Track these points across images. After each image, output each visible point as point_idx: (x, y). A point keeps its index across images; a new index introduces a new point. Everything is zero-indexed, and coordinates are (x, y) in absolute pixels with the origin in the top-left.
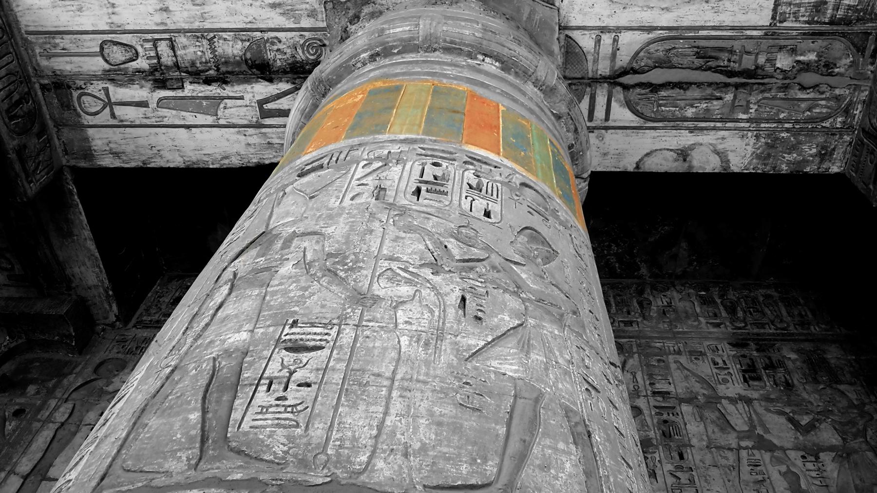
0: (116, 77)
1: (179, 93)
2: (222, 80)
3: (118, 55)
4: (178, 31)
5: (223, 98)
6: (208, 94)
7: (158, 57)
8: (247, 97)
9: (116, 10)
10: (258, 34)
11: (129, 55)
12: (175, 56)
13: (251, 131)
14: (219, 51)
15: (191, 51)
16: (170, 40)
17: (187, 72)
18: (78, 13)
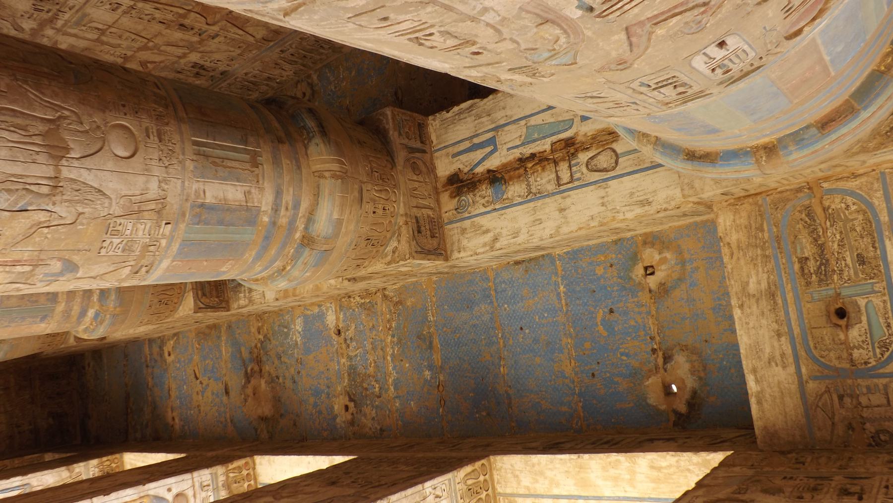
0: (607, 137)
1: (555, 138)
2: (522, 161)
3: (604, 160)
4: (553, 194)
5: (523, 144)
6: (532, 145)
7: (570, 167)
8: (505, 152)
9: (601, 201)
10: (497, 207)
11: (595, 162)
12: (556, 172)
13: (502, 122)
14: (524, 186)
15: (544, 179)
16: (559, 185)
17: (547, 159)
18: (634, 191)
